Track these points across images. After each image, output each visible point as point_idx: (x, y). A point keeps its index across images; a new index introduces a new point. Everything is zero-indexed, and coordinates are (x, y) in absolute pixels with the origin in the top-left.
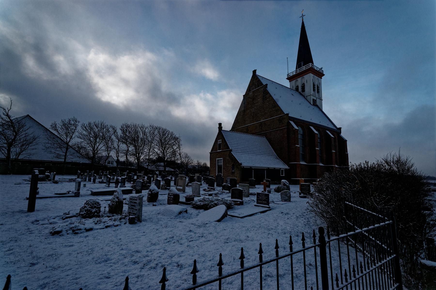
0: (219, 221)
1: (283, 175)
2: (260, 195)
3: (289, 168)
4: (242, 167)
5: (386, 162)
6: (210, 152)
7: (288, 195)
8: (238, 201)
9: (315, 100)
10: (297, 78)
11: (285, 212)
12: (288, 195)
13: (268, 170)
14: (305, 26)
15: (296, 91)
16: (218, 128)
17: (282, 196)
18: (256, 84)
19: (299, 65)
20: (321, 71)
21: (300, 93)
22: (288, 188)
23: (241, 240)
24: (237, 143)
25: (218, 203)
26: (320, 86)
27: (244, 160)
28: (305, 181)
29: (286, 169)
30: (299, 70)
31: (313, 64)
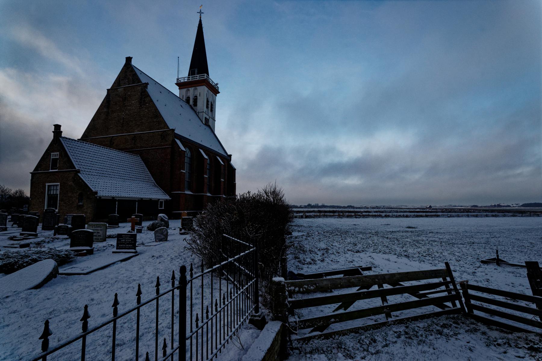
0: (38, 287)
1: (162, 208)
2: (122, 237)
3: (171, 199)
4: (98, 198)
5: (266, 192)
6: (32, 171)
7: (165, 233)
8: (83, 250)
10: (189, 87)
11: (157, 254)
12: (165, 233)
13: (141, 201)
15: (186, 103)
16: (53, 132)
17: (157, 235)
18: (130, 77)
19: (192, 72)
21: (191, 106)
22: (167, 225)
23: (78, 308)
24: (90, 160)
25: (40, 258)
26: (214, 105)
27: (102, 187)
28: (188, 214)
29: (167, 200)
30: (192, 77)
31: (209, 75)
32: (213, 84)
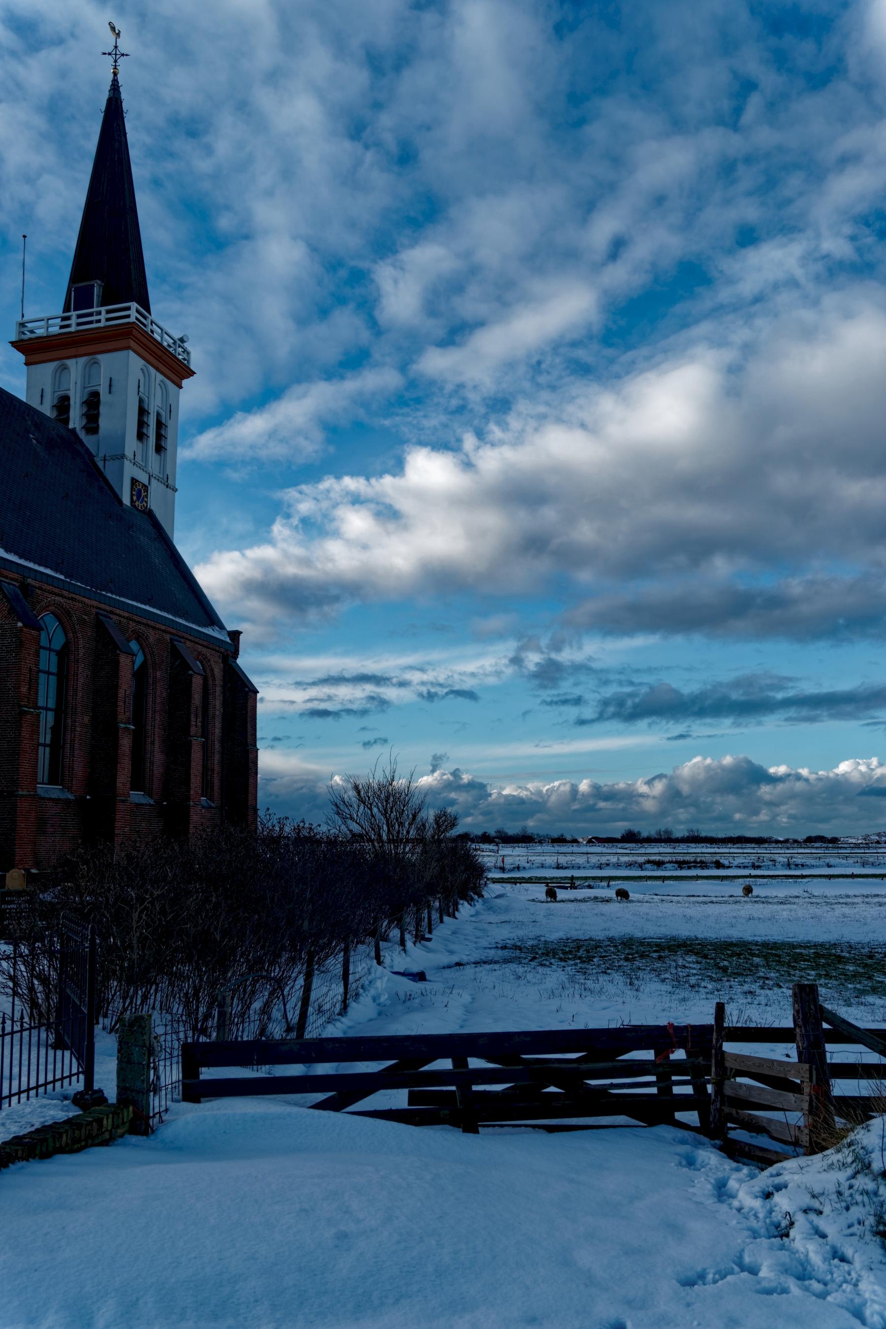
9: (144, 485)
14: (125, 106)
20: (180, 349)
26: (170, 424)
30: (79, 316)
32: (166, 341)
